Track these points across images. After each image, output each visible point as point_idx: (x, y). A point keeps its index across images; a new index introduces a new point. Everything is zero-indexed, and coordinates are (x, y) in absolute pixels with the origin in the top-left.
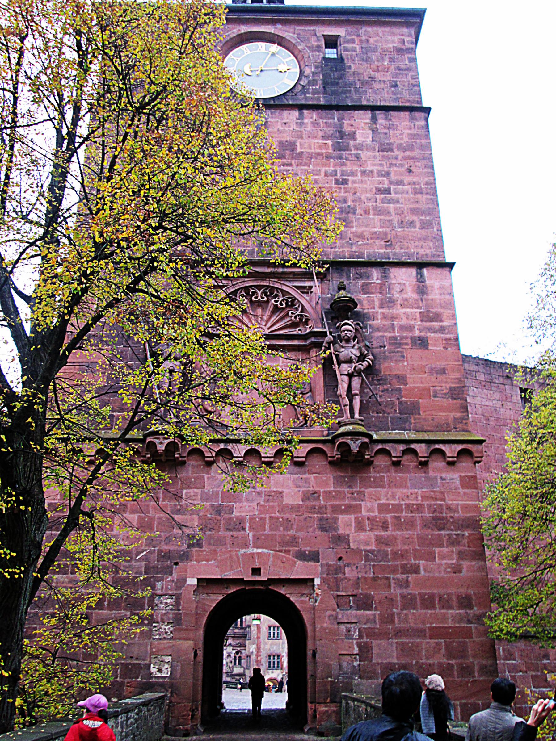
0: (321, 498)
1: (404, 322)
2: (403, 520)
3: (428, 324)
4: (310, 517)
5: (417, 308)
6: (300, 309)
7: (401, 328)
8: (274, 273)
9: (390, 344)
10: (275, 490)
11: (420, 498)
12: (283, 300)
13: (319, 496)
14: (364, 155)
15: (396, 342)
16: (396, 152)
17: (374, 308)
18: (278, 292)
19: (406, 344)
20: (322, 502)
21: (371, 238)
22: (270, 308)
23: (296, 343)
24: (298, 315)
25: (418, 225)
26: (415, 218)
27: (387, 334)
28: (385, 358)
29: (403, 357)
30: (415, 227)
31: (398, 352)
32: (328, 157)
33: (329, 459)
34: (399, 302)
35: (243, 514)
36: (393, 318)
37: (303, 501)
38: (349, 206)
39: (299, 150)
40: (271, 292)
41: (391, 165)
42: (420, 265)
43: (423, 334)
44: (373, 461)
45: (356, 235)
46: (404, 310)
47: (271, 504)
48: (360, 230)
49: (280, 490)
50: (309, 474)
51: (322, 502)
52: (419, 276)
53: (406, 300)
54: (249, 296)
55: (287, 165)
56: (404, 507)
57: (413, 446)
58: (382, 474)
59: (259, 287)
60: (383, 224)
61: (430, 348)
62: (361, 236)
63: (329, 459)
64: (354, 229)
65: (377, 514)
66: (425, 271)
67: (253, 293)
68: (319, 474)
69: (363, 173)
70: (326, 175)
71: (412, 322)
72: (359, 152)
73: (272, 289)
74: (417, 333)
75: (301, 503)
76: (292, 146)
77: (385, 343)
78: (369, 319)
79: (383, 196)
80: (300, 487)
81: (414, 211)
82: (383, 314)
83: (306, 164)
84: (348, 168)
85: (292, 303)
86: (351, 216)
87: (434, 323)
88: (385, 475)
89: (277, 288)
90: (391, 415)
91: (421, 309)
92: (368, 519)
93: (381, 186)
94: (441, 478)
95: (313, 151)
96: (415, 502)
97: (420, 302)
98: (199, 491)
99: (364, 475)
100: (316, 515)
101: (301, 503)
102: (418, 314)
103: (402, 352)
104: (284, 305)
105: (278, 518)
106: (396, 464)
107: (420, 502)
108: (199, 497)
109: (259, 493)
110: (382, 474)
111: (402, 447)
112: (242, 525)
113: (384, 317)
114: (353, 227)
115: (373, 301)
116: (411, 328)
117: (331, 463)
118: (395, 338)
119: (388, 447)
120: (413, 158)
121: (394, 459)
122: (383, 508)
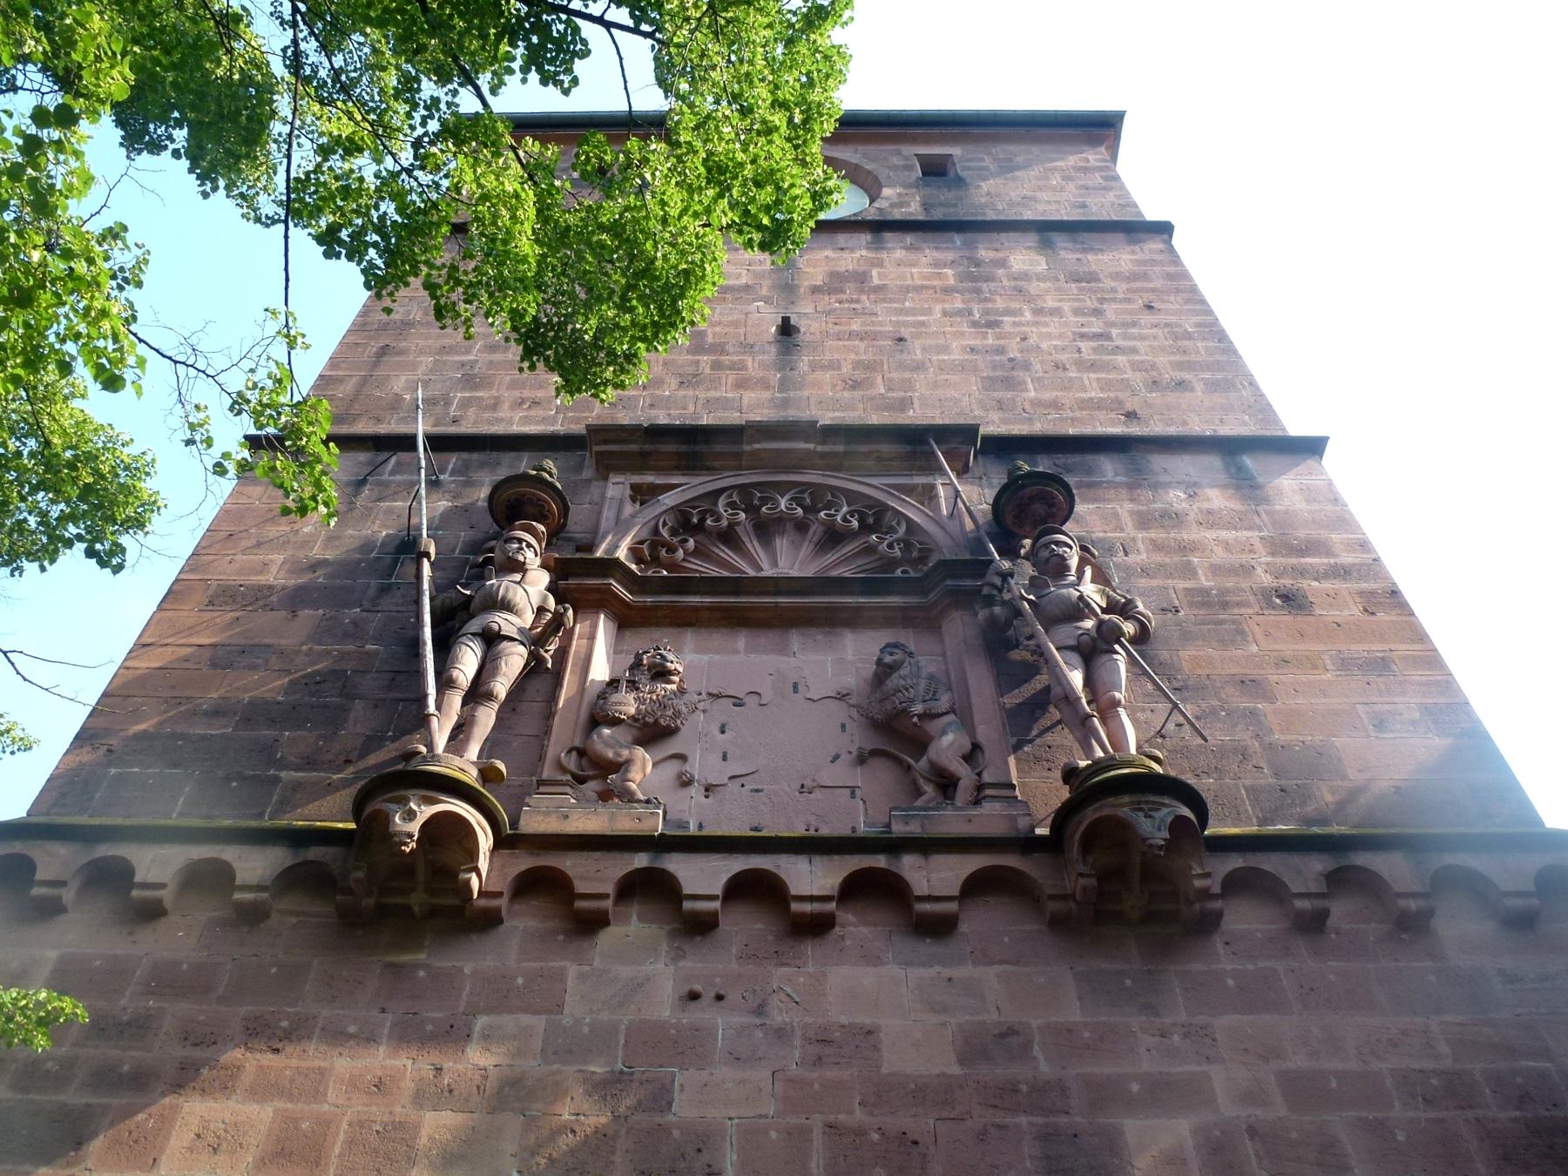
0: (1036, 1051)
1: (1220, 556)
2: (1401, 1137)
3: (1293, 561)
4: (999, 1127)
5: (1250, 528)
6: (902, 530)
7: (1216, 570)
8: (823, 455)
9: (1191, 605)
10: (844, 1020)
11: (1444, 1049)
12: (851, 513)
13: (1028, 1045)
14: (1034, 287)
15: (1212, 602)
16: (1109, 283)
17: (1122, 530)
18: (833, 495)
19: (1239, 604)
20: (1044, 1067)
21: (1081, 409)
22: (815, 530)
23: (894, 600)
24: (898, 541)
25: (1199, 387)
26: (1187, 376)
27: (1182, 585)
28: (1186, 637)
29: (1242, 633)
30: (1192, 390)
31: (1222, 622)
32: (947, 290)
33: (1053, 906)
34: (1192, 516)
35: (712, 1113)
36: (1184, 548)
37: (962, 1061)
38: (1011, 360)
39: (876, 281)
40: (816, 498)
41: (1102, 301)
42: (1229, 448)
43: (1287, 582)
44: (1219, 915)
45: (1036, 403)
46: (1210, 534)
47: (833, 1074)
48: (1047, 396)
49: (867, 1020)
50: (976, 963)
51: (1044, 1067)
52: (1233, 470)
53: (1209, 512)
54: (751, 509)
55: (852, 301)
56: (1389, 1082)
57: (1361, 859)
58: (1262, 964)
59: (783, 487)
60: (1106, 385)
61: (1318, 611)
62: (1055, 405)
63: (1053, 906)
64: (1032, 394)
65: (1283, 1112)
66: (1248, 461)
67: (764, 501)
68: (1016, 963)
69: (1038, 312)
70: (945, 313)
71: (1245, 558)
72: (1021, 283)
73: (816, 490)
74: (1266, 580)
75: (956, 1070)
76: (861, 278)
77: (1177, 603)
78: (1110, 550)
79: (1092, 344)
80: (945, 1009)
81: (1179, 366)
82: (1153, 541)
83: (891, 301)
84: (1000, 304)
85: (875, 517)
86: (1020, 374)
87: (1308, 560)
88: (1279, 966)
89: (832, 488)
90: (1248, 782)
91: (1260, 529)
92: (1252, 1131)
93: (1085, 330)
94: (1501, 972)
95: (909, 282)
96: (1428, 1065)
97: (1255, 517)
98: (539, 1023)
99: (1197, 967)
100: (1023, 1120)
101: (956, 1070)
102: (1258, 545)
103: (1233, 622)
104: (855, 524)
105: (860, 1132)
106: (1312, 925)
107: (1447, 1063)
108: (538, 1043)
109: (781, 1034)
110: (1262, 964)
111: (1318, 865)
112: (705, 1158)
113: (1157, 546)
114: (1027, 390)
115: (1116, 516)
116: (1247, 570)
117: (1060, 925)
118: (1204, 592)
119: (1268, 862)
120: (1153, 290)
121: (1301, 904)
122: (1303, 1090)
